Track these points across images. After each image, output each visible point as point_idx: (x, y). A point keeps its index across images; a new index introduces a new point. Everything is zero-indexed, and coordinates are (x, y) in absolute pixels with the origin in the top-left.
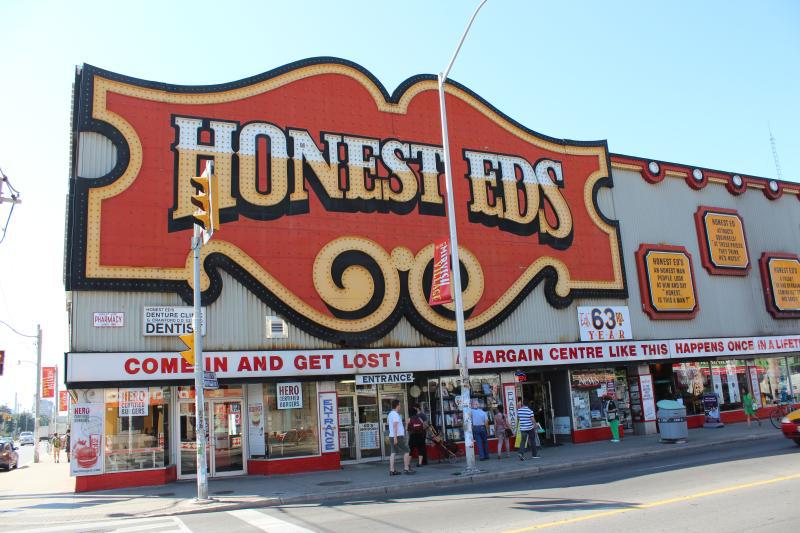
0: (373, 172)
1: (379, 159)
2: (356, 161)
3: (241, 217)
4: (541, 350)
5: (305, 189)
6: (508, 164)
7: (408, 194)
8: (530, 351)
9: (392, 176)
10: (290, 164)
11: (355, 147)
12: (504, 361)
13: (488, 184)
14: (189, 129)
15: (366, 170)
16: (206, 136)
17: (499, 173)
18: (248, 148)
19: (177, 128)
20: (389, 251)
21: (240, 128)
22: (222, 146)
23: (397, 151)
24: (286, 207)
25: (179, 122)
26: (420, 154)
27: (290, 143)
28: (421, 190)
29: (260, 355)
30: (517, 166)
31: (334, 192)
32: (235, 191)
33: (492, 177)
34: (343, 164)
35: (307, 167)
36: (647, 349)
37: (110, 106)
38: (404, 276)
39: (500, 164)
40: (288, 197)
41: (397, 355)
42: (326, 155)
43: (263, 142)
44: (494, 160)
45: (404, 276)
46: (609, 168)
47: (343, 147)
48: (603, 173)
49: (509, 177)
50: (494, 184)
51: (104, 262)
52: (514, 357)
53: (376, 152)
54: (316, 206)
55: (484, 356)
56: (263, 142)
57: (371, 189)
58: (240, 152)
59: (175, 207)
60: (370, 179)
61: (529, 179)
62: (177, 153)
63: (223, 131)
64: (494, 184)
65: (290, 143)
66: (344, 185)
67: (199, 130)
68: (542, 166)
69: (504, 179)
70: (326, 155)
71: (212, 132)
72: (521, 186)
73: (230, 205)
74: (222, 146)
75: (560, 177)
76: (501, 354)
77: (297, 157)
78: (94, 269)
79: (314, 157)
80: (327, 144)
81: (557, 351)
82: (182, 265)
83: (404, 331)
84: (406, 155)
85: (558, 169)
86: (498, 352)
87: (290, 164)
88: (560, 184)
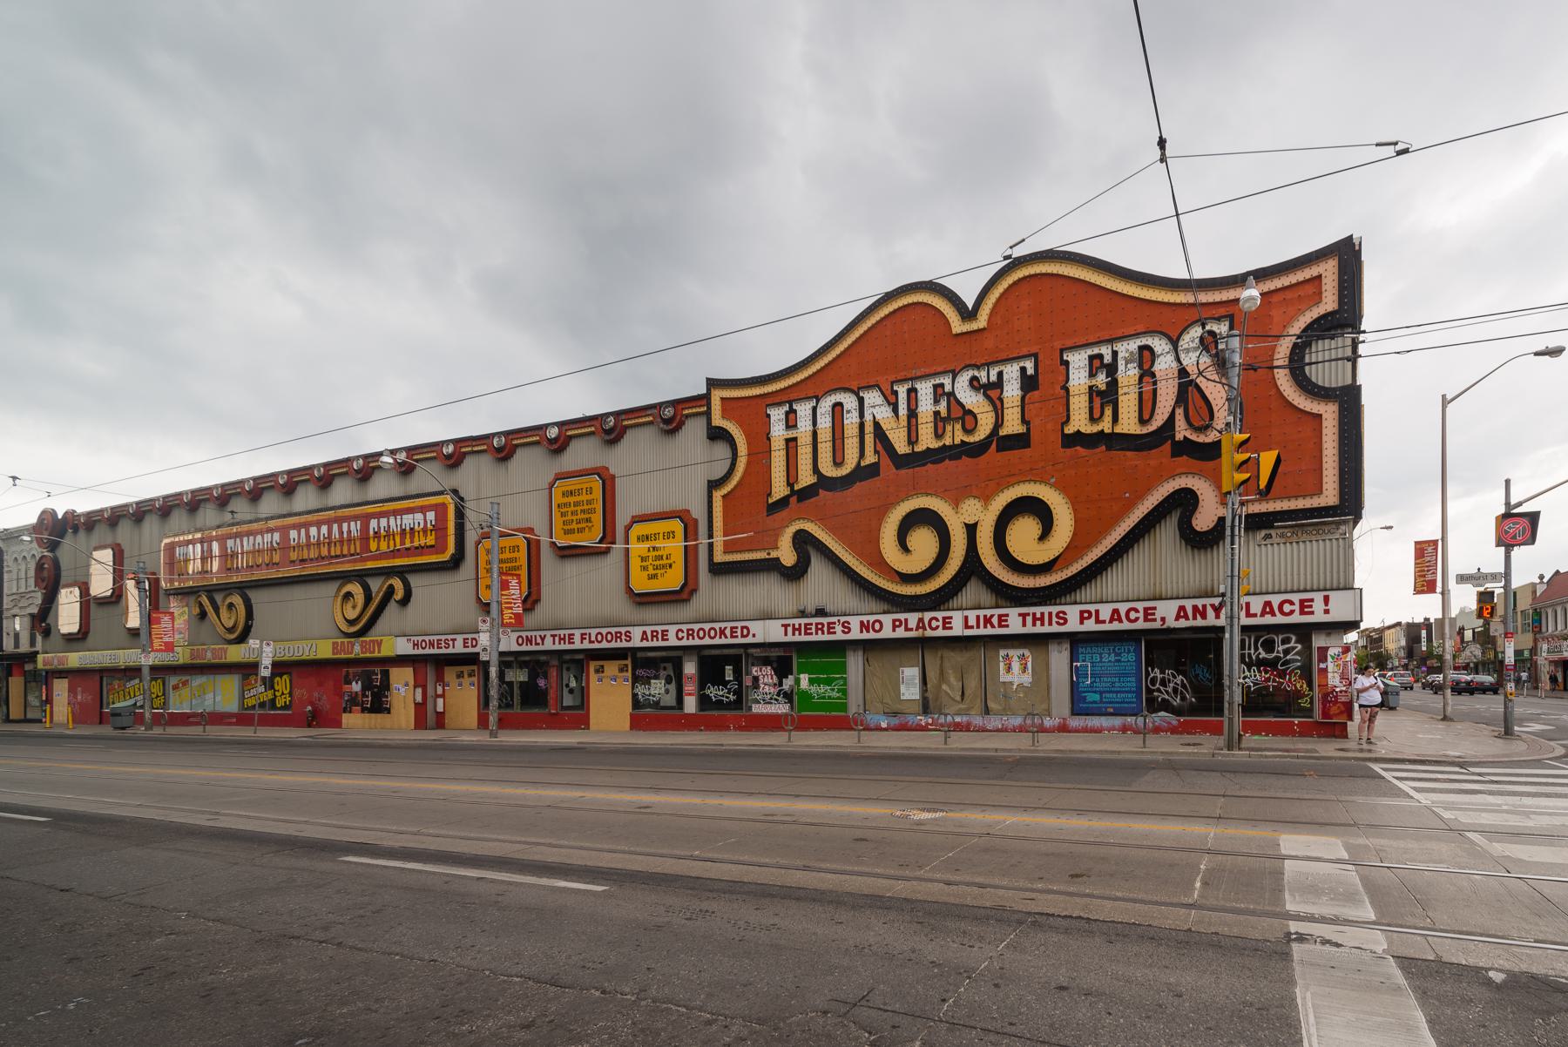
29: (1199, 603)
36: (790, 629)
41: (1326, 600)
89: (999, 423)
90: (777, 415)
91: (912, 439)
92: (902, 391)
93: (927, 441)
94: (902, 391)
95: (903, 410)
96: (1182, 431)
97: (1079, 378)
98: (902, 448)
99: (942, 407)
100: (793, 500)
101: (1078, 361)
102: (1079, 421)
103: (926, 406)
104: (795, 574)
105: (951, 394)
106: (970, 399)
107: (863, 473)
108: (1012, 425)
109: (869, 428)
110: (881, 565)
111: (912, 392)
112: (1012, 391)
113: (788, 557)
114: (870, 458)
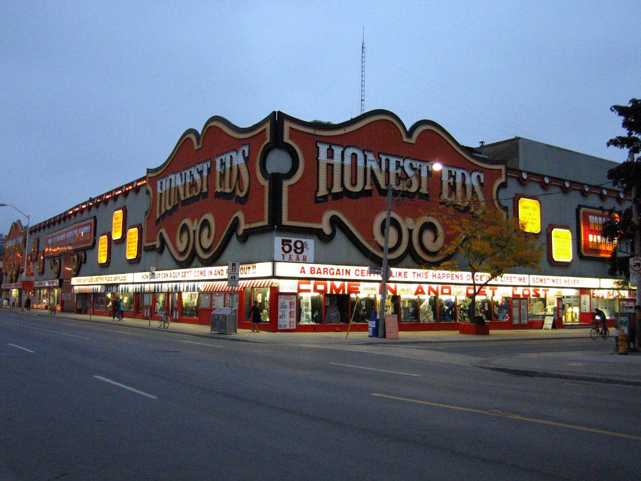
0: (400, 176)
1: (403, 168)
2: (392, 168)
3: (344, 197)
4: (349, 270)
5: (371, 184)
6: (459, 173)
7: (414, 189)
8: (343, 270)
9: (407, 177)
10: (365, 169)
11: (393, 161)
12: (327, 274)
13: (449, 183)
14: (323, 149)
15: (397, 174)
16: (330, 155)
17: (454, 177)
18: (348, 161)
19: (318, 148)
20: (404, 218)
21: (344, 149)
22: (337, 159)
23: (411, 164)
24: (365, 193)
25: (319, 145)
26: (420, 165)
27: (365, 156)
28: (420, 187)
30: (463, 174)
31: (383, 187)
32: (342, 185)
33: (452, 180)
34: (387, 171)
35: (372, 172)
37: (290, 137)
38: (410, 231)
39: (455, 172)
40: (364, 188)
42: (380, 164)
43: (354, 156)
44: (453, 170)
45: (410, 231)
46: (507, 176)
47: (387, 160)
48: (503, 180)
49: (459, 180)
50: (452, 184)
51: (289, 219)
52: (334, 272)
53: (401, 164)
54: (376, 193)
55: (316, 271)
56: (354, 156)
57: (398, 185)
58: (344, 162)
59: (317, 191)
60: (399, 178)
61: (468, 182)
62: (318, 161)
63: (337, 151)
64: (452, 184)
65: (365, 156)
66: (387, 183)
67: (328, 149)
68: (475, 175)
69: (456, 181)
70: (380, 164)
71: (333, 150)
72: (464, 185)
73: (340, 191)
74: (337, 159)
75: (482, 181)
76: (326, 270)
77: (368, 166)
78: (285, 222)
79: (375, 166)
80: (380, 159)
81: (359, 271)
82: (320, 221)
83: (409, 259)
84: (414, 166)
85: (482, 176)
86: (324, 269)
87: (365, 169)
88: (481, 184)
89: (202, 189)
90: (159, 183)
91: (185, 195)
92: (183, 173)
93: (188, 196)
94: (183, 173)
95: (183, 183)
96: (238, 193)
97: (218, 168)
98: (182, 198)
99: (191, 182)
100: (161, 219)
101: (218, 161)
102: (219, 190)
103: (188, 180)
104: (161, 251)
105: (193, 175)
106: (197, 177)
107: (175, 207)
108: (205, 190)
109: (176, 188)
110: (176, 248)
111: (185, 174)
112: (205, 174)
113: (158, 243)
114: (176, 203)
